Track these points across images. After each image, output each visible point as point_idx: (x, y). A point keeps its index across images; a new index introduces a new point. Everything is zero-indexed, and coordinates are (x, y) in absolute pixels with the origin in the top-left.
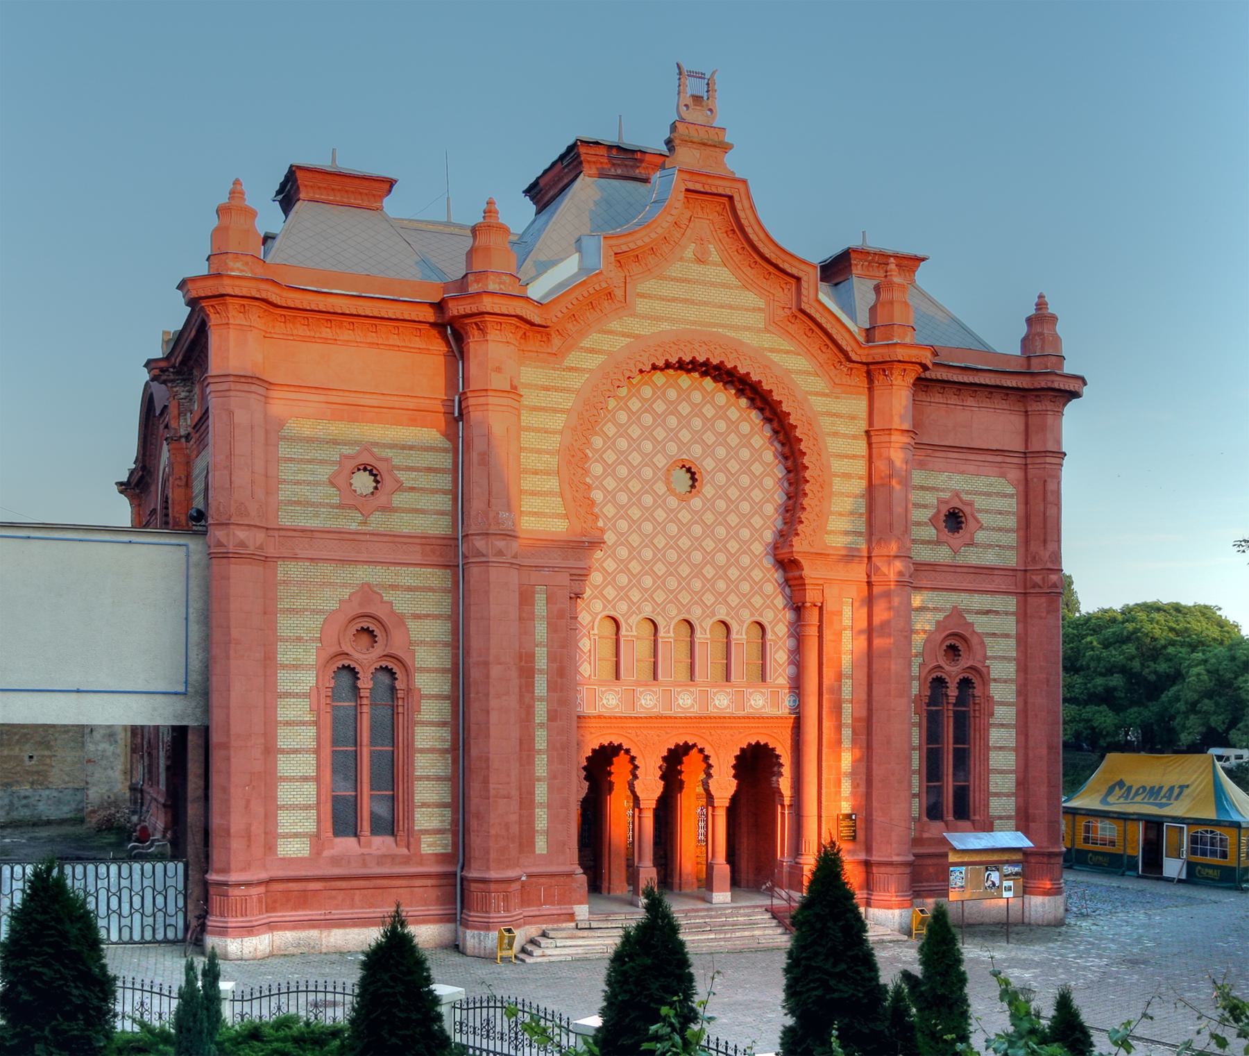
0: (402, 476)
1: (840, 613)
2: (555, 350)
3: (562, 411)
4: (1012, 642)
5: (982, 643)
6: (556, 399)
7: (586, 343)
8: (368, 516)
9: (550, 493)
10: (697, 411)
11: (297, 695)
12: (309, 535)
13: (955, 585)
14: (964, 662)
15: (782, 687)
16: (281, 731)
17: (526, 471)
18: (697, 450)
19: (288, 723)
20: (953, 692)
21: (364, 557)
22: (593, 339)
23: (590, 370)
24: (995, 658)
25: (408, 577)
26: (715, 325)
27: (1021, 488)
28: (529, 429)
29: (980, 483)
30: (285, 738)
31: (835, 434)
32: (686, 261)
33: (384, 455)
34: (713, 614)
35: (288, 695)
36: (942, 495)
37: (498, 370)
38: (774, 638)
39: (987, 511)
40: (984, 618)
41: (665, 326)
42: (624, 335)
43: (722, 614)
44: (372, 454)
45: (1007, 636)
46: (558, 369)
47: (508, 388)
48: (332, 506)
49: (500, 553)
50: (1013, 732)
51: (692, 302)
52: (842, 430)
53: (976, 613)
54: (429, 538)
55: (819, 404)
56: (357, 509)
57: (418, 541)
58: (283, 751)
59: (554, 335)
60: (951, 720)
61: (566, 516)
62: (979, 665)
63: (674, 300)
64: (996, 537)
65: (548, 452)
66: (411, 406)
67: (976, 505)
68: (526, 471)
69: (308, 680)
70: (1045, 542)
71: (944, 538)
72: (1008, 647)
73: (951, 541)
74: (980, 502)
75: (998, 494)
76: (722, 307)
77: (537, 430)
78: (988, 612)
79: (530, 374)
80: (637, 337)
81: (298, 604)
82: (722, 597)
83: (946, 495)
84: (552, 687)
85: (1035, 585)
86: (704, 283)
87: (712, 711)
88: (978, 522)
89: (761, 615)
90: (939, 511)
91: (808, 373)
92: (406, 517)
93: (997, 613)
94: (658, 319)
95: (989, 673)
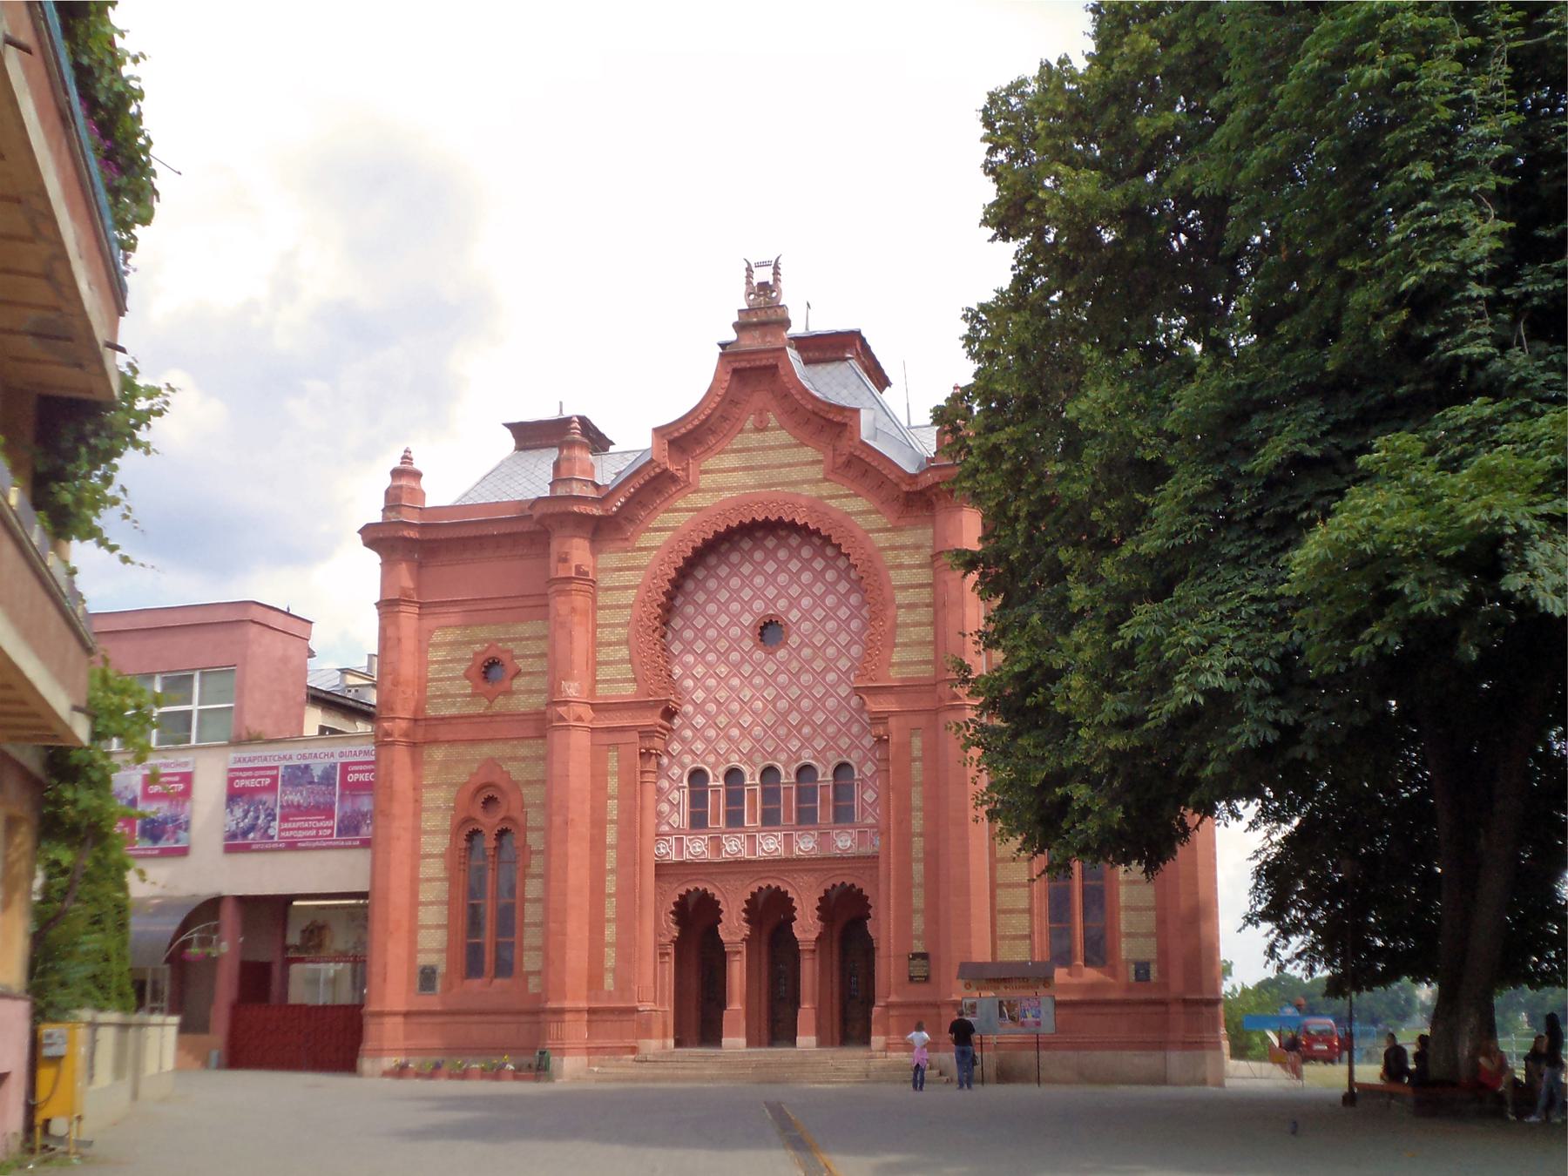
0: (521, 664)
7: (655, 524)
9: (622, 661)
10: (782, 567)
15: (871, 826)
16: (423, 887)
17: (601, 644)
19: (428, 880)
22: (662, 519)
23: (659, 547)
25: (523, 751)
28: (603, 608)
31: (900, 566)
34: (799, 758)
41: (727, 495)
42: (688, 510)
43: (807, 758)
47: (573, 575)
48: (465, 696)
49: (562, 718)
52: (906, 561)
55: (881, 540)
57: (531, 717)
59: (623, 522)
65: (619, 625)
68: (601, 644)
77: (610, 607)
80: (698, 510)
82: (807, 742)
84: (621, 835)
86: (763, 449)
89: (849, 756)
91: (869, 512)
92: (523, 697)
94: (720, 489)
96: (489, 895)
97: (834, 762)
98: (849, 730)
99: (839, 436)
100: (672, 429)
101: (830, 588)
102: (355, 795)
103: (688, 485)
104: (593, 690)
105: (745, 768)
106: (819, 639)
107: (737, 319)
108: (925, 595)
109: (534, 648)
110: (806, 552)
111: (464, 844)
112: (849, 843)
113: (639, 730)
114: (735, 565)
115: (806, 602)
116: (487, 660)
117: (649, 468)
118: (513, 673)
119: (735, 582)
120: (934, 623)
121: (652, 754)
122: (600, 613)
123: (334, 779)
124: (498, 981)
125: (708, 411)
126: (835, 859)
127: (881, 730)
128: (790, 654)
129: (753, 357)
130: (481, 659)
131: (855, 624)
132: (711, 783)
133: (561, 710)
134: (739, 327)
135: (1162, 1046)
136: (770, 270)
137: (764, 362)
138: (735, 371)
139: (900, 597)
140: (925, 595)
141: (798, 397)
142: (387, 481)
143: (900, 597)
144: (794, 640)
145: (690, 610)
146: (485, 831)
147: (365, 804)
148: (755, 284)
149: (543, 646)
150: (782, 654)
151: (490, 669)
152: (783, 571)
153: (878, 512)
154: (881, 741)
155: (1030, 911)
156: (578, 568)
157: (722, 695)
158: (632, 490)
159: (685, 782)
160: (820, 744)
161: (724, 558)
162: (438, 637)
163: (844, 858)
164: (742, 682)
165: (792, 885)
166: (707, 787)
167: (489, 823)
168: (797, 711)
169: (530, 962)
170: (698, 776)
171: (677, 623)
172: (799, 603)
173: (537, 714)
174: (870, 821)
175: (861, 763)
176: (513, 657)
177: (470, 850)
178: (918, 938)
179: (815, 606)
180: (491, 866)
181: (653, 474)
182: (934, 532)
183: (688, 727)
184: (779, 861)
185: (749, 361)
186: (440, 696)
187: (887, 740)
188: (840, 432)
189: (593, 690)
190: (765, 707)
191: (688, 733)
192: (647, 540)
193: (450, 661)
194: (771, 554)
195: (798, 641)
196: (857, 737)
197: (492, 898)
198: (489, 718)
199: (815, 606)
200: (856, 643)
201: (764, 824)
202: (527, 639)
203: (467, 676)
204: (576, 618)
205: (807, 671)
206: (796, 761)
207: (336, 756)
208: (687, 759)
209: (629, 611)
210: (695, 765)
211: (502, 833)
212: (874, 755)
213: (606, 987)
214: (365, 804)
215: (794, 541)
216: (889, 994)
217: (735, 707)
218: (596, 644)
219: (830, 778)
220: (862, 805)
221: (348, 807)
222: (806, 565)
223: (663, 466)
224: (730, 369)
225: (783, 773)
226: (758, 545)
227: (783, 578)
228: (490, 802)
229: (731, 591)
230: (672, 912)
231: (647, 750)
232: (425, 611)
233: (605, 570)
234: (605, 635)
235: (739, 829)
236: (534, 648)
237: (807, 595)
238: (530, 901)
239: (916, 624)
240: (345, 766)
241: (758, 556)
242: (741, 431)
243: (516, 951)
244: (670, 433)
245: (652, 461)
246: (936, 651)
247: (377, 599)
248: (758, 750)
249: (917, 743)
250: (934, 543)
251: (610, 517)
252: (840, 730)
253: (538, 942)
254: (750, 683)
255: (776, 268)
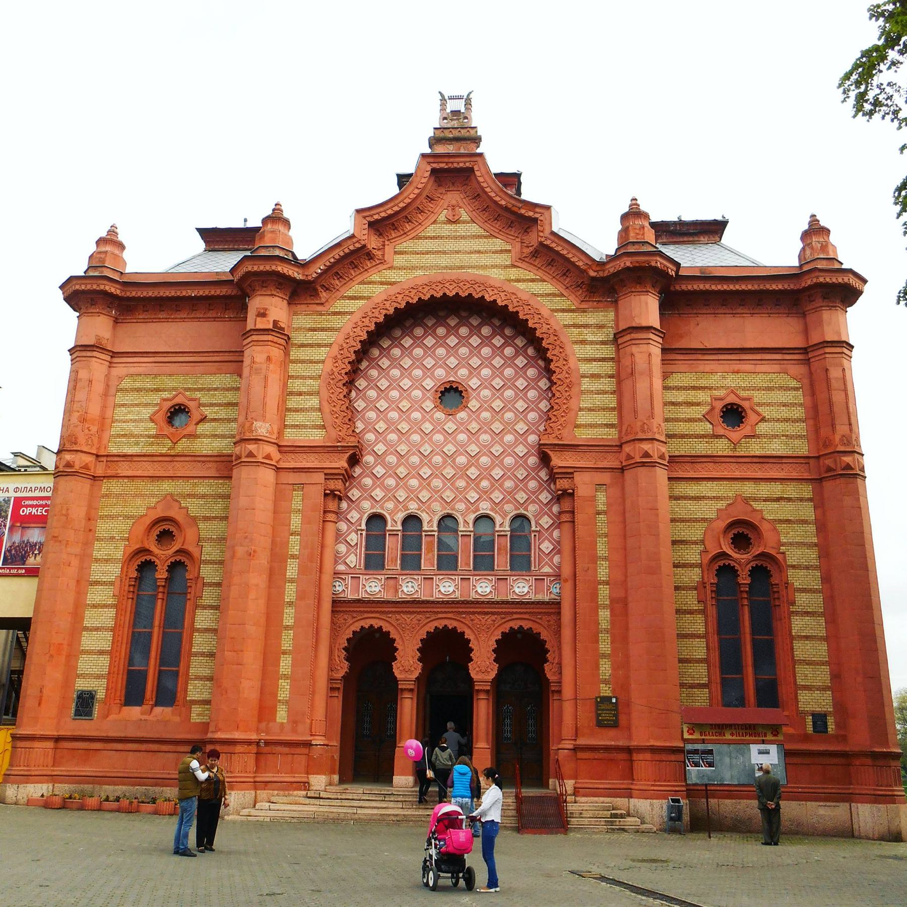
0: (208, 412)
1: (593, 499)
2: (323, 300)
3: (326, 346)
4: (812, 528)
5: (775, 528)
6: (321, 336)
8: (176, 443)
9: (312, 409)
10: (463, 341)
11: (104, 583)
12: (129, 459)
13: (737, 474)
14: (756, 550)
16: (88, 613)
17: (291, 393)
18: (463, 372)
19: (94, 606)
20: (744, 579)
21: (171, 473)
22: (356, 289)
23: (352, 313)
24: (791, 544)
25: (203, 488)
26: (462, 267)
27: (806, 381)
29: (759, 380)
30: (91, 618)
31: (583, 342)
32: (439, 223)
33: (194, 396)
34: (477, 510)
35: (97, 583)
36: (717, 393)
37: (262, 314)
38: (538, 529)
39: (769, 405)
40: (775, 505)
41: (420, 273)
42: (382, 283)
43: (485, 507)
44: (183, 395)
45: (804, 522)
46: (324, 315)
47: (271, 326)
48: (149, 436)
49: (251, 454)
50: (822, 620)
51: (444, 253)
52: (590, 338)
53: (764, 501)
54: (224, 456)
56: (169, 438)
57: (211, 459)
58: (87, 629)
60: (746, 610)
61: (324, 427)
62: (773, 552)
63: (427, 253)
64: (780, 427)
65: (311, 378)
66: (218, 359)
67: (756, 400)
68: (291, 393)
69: (113, 571)
70: (833, 426)
71: (720, 431)
72: (809, 533)
73: (727, 433)
74: (758, 397)
75: (781, 388)
76: (471, 253)
77: (303, 362)
78: (778, 499)
79: (303, 320)
81: (114, 511)
82: (485, 494)
83: (721, 393)
85: (829, 469)
86: (455, 238)
87: (473, 596)
88: (758, 414)
89: (526, 509)
90: (713, 409)
91: (554, 295)
93: (789, 500)
95: (785, 557)
96: (157, 623)
97: (512, 514)
98: (526, 485)
99: (526, 231)
100: (372, 212)
101: (509, 362)
102: (23, 528)
103: (383, 262)
104: (280, 433)
105: (425, 517)
106: (497, 404)
107: (433, 135)
108: (608, 368)
109: (220, 398)
110: (486, 331)
111: (135, 574)
112: (526, 590)
113: (326, 471)
114: (418, 338)
115: (486, 372)
116: (173, 406)
117: (349, 242)
118: (199, 418)
119: (418, 352)
120: (618, 392)
121: (335, 495)
122: (291, 366)
123: (6, 511)
124: (158, 710)
125: (408, 201)
126: (513, 603)
127: (563, 484)
128: (470, 416)
129: (451, 160)
130: (170, 404)
131: (532, 394)
132: (389, 527)
133: (252, 447)
134: (434, 141)
135: (848, 798)
136: (463, 102)
137: (461, 165)
138: (434, 171)
139: (585, 368)
140: (608, 368)
141: (492, 194)
142: (93, 248)
143: (585, 368)
144: (473, 404)
145: (374, 373)
146: (157, 562)
147: (35, 535)
148: (448, 110)
149: (230, 397)
150: (462, 415)
151: (177, 412)
152: (464, 345)
153: (562, 295)
154: (564, 496)
155: (706, 661)
156: (275, 323)
157: (403, 449)
158: (332, 260)
159: (364, 527)
160: (497, 496)
161: (408, 331)
162: (126, 383)
163: (523, 603)
164: (422, 438)
165: (469, 627)
166: (385, 530)
167: (163, 555)
168: (476, 467)
169: (196, 691)
170: (376, 519)
171: (361, 383)
172: (479, 373)
173: (220, 456)
174: (547, 569)
175: (538, 516)
176: (200, 405)
177: (139, 580)
178: (606, 682)
179: (494, 376)
180: (160, 596)
181: (352, 248)
182: (617, 315)
183: (367, 476)
184: (458, 602)
185: (447, 163)
186: (124, 436)
187: (572, 495)
188: (529, 228)
189: (280, 433)
190: (445, 462)
191: (368, 481)
192: (340, 305)
193: (137, 405)
194: (452, 330)
195: (478, 405)
196: (534, 493)
197: (160, 627)
198: (172, 457)
199: (494, 376)
200: (533, 410)
201: (439, 568)
202: (216, 389)
203: (152, 420)
204: (272, 366)
205: (485, 432)
206: (474, 513)
207: (11, 490)
208: (366, 505)
209: (321, 366)
210: (374, 511)
211: (175, 567)
212: (550, 510)
213: (278, 720)
214: (35, 535)
215: (475, 322)
216: (577, 736)
217: (415, 459)
218: (286, 393)
219: (508, 528)
220: (539, 554)
221: (17, 538)
222: (486, 341)
223: (363, 243)
224: (429, 168)
225: (461, 520)
226: (442, 321)
227: (463, 351)
228: (165, 536)
229: (415, 360)
230: (345, 649)
231: (332, 491)
232: (115, 360)
233: (298, 329)
234: (295, 385)
235: (418, 572)
236: (220, 398)
237: (487, 366)
238: (198, 630)
239: (599, 392)
240: (18, 502)
241: (441, 331)
242: (435, 222)
243: (181, 680)
244: (371, 216)
245: (353, 236)
246: (620, 417)
247: (72, 345)
248: (436, 500)
249: (601, 498)
250: (617, 325)
251: (309, 282)
252: (517, 486)
253: (206, 672)
254: (431, 439)
255: (468, 102)
